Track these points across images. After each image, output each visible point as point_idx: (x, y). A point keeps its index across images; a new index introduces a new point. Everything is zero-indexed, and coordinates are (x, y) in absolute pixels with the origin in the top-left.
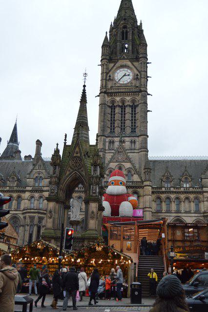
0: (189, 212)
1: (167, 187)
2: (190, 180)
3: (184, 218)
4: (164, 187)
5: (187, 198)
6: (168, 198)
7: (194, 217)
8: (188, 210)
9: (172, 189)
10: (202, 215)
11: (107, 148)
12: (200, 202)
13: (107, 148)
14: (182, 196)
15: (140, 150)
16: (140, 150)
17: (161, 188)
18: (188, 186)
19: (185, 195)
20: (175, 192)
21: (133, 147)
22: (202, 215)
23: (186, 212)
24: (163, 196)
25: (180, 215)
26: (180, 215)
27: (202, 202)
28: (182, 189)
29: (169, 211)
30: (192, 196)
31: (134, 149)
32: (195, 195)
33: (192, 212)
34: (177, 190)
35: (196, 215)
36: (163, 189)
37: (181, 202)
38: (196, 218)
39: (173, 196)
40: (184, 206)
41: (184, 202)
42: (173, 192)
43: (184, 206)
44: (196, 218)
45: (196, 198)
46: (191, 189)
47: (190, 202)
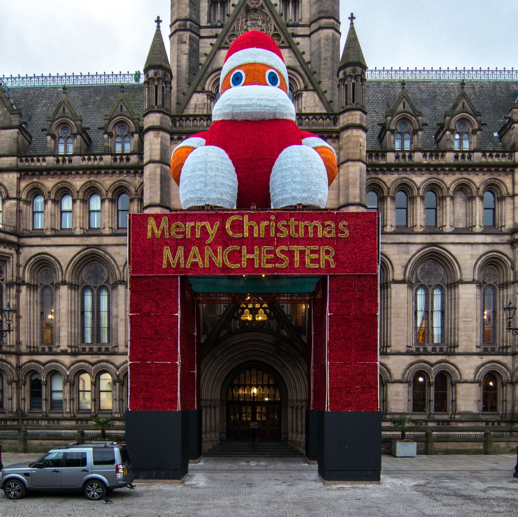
0: (468, 231)
1: (403, 151)
2: (476, 126)
3: (450, 248)
4: (393, 151)
5: (463, 188)
6: (405, 187)
7: (481, 247)
8: (461, 225)
9: (418, 157)
10: (506, 238)
11: (204, 21)
12: (502, 199)
13: (204, 21)
14: (449, 180)
15: (314, 27)
16: (314, 27)
17: (383, 153)
18: (466, 146)
19: (458, 176)
20: (427, 168)
21: (290, 15)
22: (506, 238)
23: (457, 232)
24: (389, 179)
25: (438, 238)
26: (438, 238)
27: (509, 200)
28: (449, 157)
29: (405, 229)
30: (478, 180)
31: (298, 26)
32: (487, 177)
33: (477, 229)
34: (434, 161)
35: (489, 239)
36: (391, 157)
37: (443, 198)
38: (487, 249)
39: (419, 180)
40: (453, 213)
41: (452, 198)
42: (420, 168)
43: (453, 212)
44: (487, 249)
45: (492, 187)
46: (477, 157)
47: (471, 198)
